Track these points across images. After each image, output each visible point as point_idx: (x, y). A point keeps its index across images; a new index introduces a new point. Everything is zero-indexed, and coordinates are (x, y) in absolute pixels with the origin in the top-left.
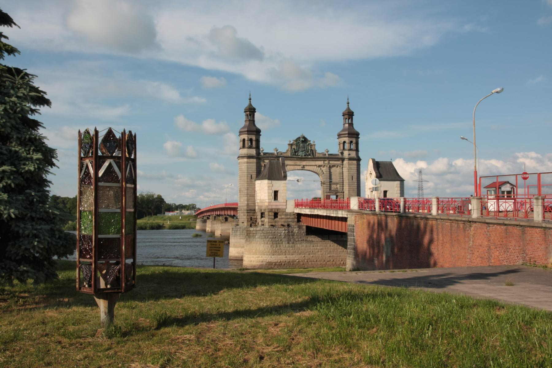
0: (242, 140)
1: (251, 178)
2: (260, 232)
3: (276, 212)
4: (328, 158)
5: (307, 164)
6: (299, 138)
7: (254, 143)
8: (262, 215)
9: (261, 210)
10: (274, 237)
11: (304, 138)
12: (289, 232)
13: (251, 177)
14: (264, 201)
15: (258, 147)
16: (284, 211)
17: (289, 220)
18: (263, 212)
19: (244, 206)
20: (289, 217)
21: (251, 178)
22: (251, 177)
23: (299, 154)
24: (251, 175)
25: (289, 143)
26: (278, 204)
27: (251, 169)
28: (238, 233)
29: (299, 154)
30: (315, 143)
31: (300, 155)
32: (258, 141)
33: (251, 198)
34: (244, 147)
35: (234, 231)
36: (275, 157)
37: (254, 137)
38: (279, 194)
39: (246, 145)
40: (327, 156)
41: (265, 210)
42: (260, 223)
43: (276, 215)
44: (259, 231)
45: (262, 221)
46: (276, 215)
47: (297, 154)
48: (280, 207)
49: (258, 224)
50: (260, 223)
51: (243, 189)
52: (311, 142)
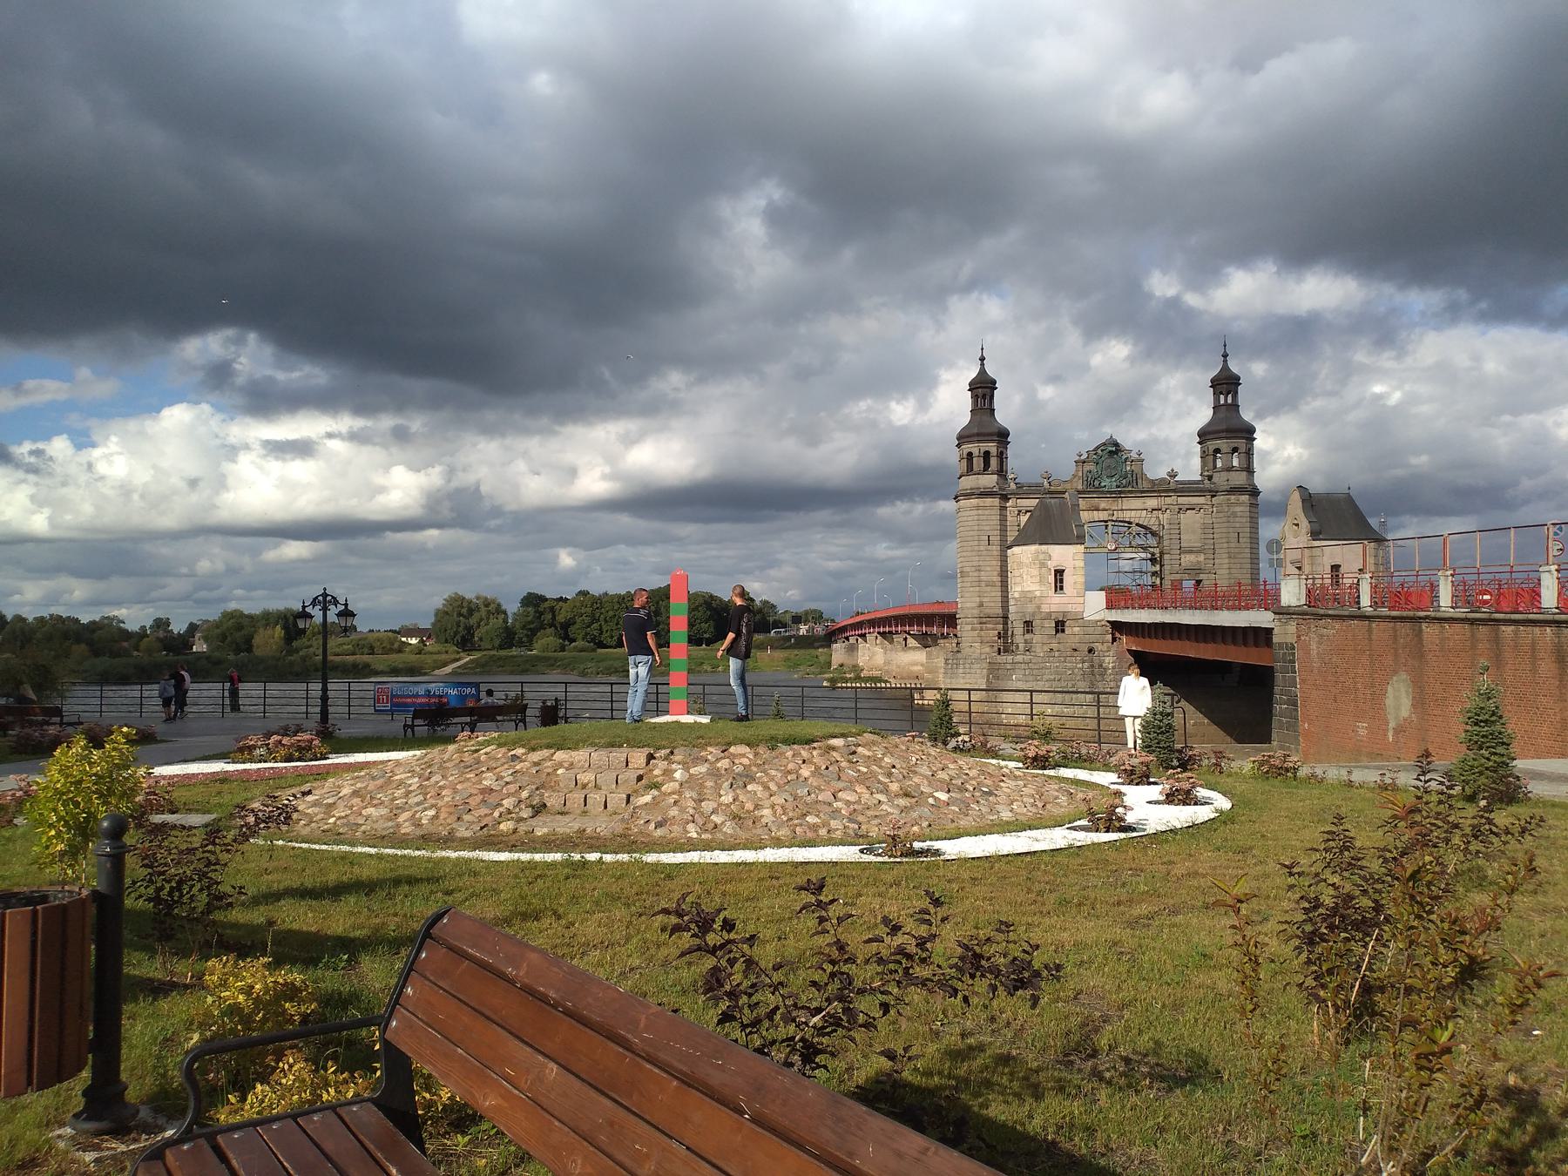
0: (965, 456)
4: (1174, 491)
6: (1104, 444)
7: (994, 462)
8: (1028, 625)
10: (1058, 677)
11: (1116, 444)
12: (1092, 666)
15: (1001, 472)
16: (1078, 619)
17: (1092, 638)
19: (973, 608)
20: (1091, 630)
23: (1103, 484)
26: (1065, 600)
27: (988, 523)
28: (961, 671)
29: (1103, 484)
32: (1002, 457)
33: (989, 589)
34: (970, 470)
36: (1048, 492)
37: (992, 447)
38: (1066, 576)
39: (975, 468)
40: (1172, 486)
41: (1033, 614)
42: (1021, 646)
43: (1060, 626)
46: (1060, 626)
47: (1096, 483)
48: (1069, 608)
49: (1017, 647)
50: (1021, 646)
51: (968, 569)
52: (1134, 455)
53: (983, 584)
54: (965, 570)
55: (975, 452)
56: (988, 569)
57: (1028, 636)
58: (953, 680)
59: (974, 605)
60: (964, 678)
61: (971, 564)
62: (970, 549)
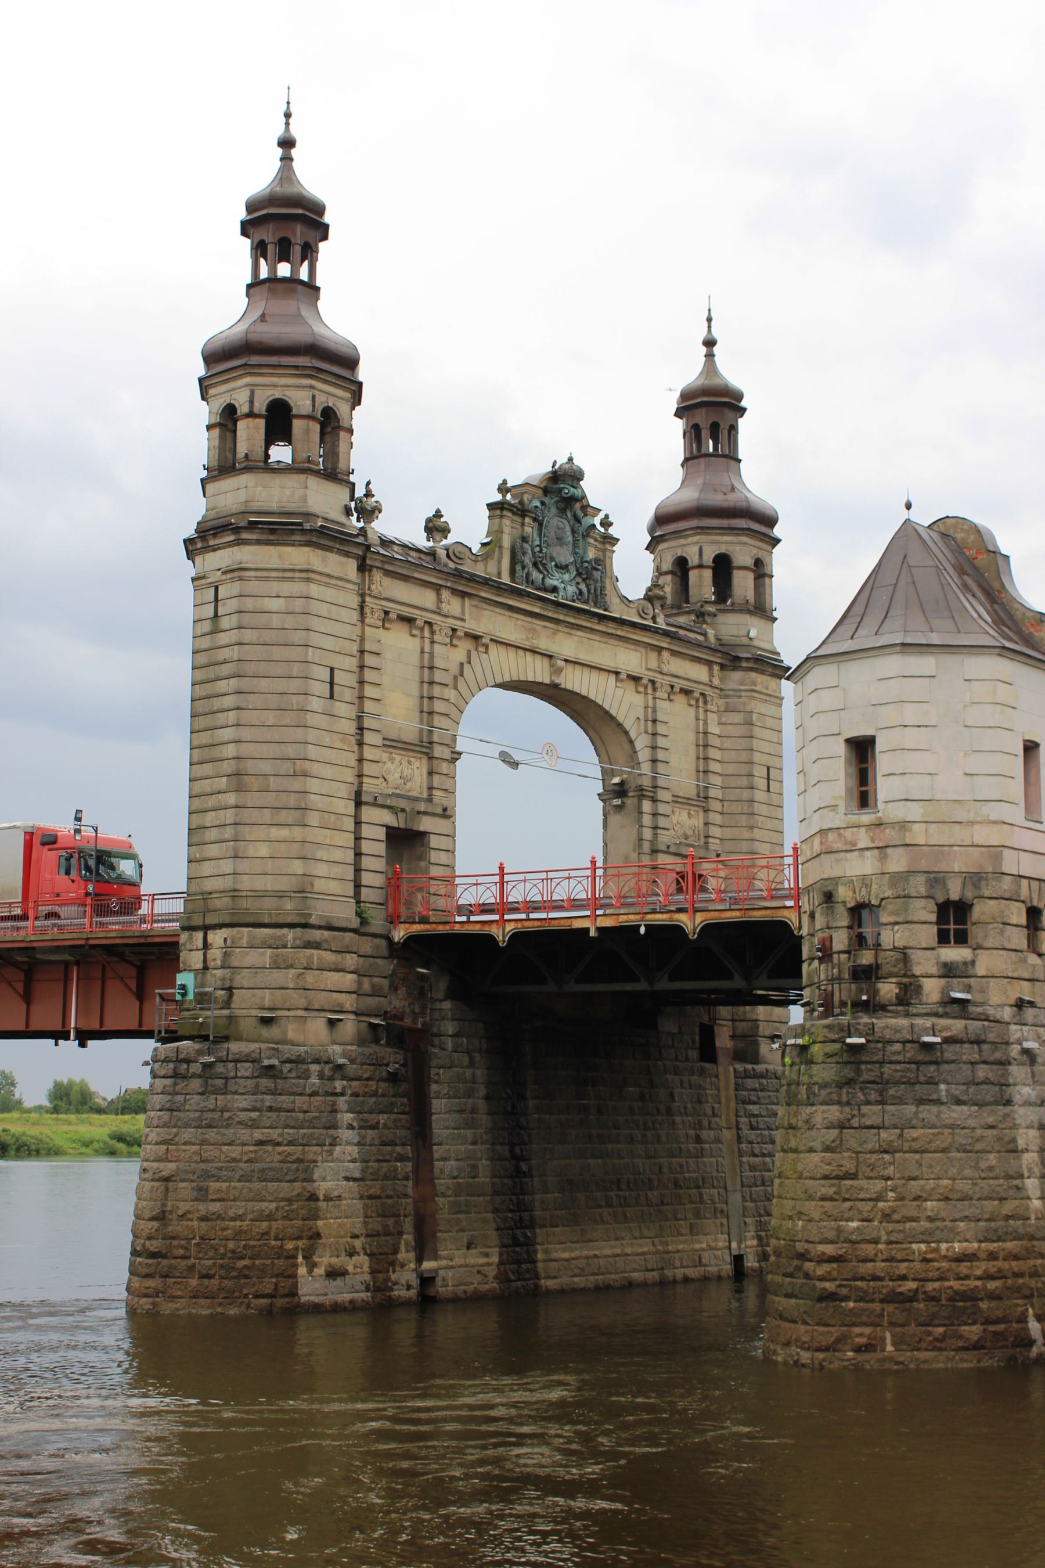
1: (332, 697)
2: (968, 1052)
3: (1035, 903)
5: (583, 657)
9: (936, 880)
13: (332, 683)
14: (961, 815)
18: (955, 896)
19: (280, 895)
21: (332, 697)
22: (332, 683)
23: (551, 582)
24: (332, 670)
25: (498, 497)
28: (242, 1102)
30: (611, 531)
31: (554, 590)
35: (196, 1084)
41: (975, 879)
44: (961, 1042)
45: (949, 971)
50: (932, 989)
51: (267, 767)
53: (313, 819)
54: (250, 766)
55: (300, 400)
56: (327, 771)
57: (953, 954)
58: (212, 1134)
59: (284, 884)
60: (254, 1125)
61: (274, 750)
62: (274, 701)
